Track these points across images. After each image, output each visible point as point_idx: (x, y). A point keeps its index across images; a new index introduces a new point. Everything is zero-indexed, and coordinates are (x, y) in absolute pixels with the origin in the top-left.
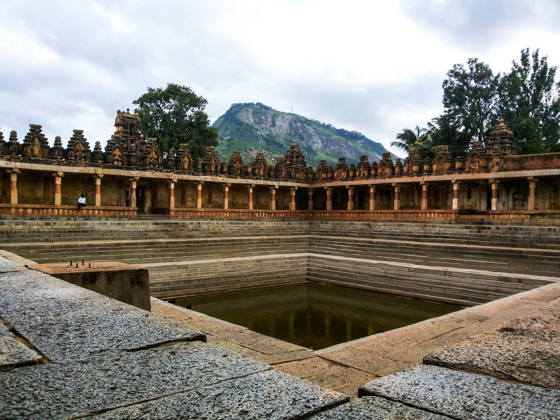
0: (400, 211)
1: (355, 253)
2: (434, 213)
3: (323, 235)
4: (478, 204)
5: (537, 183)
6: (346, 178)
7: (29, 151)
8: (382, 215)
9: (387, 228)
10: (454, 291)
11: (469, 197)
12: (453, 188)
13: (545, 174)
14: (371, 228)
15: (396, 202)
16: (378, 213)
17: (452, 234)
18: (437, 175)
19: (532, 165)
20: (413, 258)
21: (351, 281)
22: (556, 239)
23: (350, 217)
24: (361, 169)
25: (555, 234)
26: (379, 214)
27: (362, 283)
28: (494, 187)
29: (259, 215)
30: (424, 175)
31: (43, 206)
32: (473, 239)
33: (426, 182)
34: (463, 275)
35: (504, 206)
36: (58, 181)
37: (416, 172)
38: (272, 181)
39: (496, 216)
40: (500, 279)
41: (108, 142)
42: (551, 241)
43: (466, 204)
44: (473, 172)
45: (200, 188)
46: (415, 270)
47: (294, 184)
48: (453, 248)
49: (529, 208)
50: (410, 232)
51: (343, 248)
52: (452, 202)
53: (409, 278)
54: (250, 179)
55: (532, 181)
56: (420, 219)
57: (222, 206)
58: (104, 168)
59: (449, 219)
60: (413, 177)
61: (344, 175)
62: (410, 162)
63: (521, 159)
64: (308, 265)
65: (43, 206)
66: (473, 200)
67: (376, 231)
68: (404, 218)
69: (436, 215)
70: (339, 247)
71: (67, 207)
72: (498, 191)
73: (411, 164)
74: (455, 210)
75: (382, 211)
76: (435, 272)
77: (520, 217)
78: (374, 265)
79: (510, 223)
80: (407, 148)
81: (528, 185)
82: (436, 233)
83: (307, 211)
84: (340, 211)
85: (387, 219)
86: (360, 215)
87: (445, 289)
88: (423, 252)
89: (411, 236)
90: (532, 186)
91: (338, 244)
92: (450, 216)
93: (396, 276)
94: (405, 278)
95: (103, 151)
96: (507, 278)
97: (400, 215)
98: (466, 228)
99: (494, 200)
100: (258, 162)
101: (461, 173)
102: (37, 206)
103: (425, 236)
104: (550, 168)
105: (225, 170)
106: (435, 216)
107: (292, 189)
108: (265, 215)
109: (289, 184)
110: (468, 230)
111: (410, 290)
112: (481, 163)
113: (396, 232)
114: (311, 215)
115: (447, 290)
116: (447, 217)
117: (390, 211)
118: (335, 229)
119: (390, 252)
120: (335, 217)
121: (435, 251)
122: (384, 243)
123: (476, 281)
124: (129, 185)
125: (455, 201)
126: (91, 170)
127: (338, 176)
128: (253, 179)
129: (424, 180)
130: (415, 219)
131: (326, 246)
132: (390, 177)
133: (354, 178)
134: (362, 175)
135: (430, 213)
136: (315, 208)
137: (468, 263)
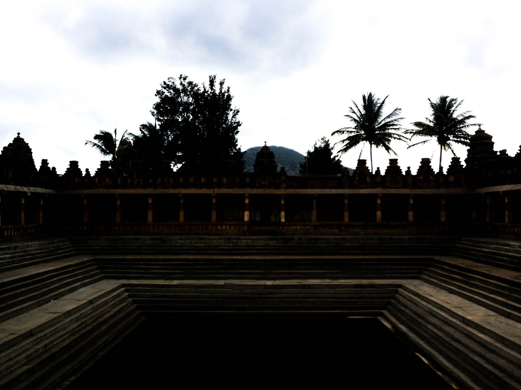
2: (226, 225)
8: (164, 228)
18: (228, 188)
26: (161, 227)
29: (7, 233)
30: (214, 188)
33: (217, 194)
39: (285, 228)
40: (355, 286)
46: (272, 287)
47: (44, 191)
50: (217, 246)
51: (153, 269)
52: (244, 214)
60: (201, 188)
64: (129, 296)
67: (175, 246)
69: (228, 227)
74: (247, 222)
80: (102, 150)
82: (245, 246)
90: (314, 202)
93: (257, 296)
98: (271, 239)
99: (283, 214)
108: (14, 233)
110: (275, 242)
113: (200, 246)
125: (247, 214)
133: (124, 186)
135: (222, 225)
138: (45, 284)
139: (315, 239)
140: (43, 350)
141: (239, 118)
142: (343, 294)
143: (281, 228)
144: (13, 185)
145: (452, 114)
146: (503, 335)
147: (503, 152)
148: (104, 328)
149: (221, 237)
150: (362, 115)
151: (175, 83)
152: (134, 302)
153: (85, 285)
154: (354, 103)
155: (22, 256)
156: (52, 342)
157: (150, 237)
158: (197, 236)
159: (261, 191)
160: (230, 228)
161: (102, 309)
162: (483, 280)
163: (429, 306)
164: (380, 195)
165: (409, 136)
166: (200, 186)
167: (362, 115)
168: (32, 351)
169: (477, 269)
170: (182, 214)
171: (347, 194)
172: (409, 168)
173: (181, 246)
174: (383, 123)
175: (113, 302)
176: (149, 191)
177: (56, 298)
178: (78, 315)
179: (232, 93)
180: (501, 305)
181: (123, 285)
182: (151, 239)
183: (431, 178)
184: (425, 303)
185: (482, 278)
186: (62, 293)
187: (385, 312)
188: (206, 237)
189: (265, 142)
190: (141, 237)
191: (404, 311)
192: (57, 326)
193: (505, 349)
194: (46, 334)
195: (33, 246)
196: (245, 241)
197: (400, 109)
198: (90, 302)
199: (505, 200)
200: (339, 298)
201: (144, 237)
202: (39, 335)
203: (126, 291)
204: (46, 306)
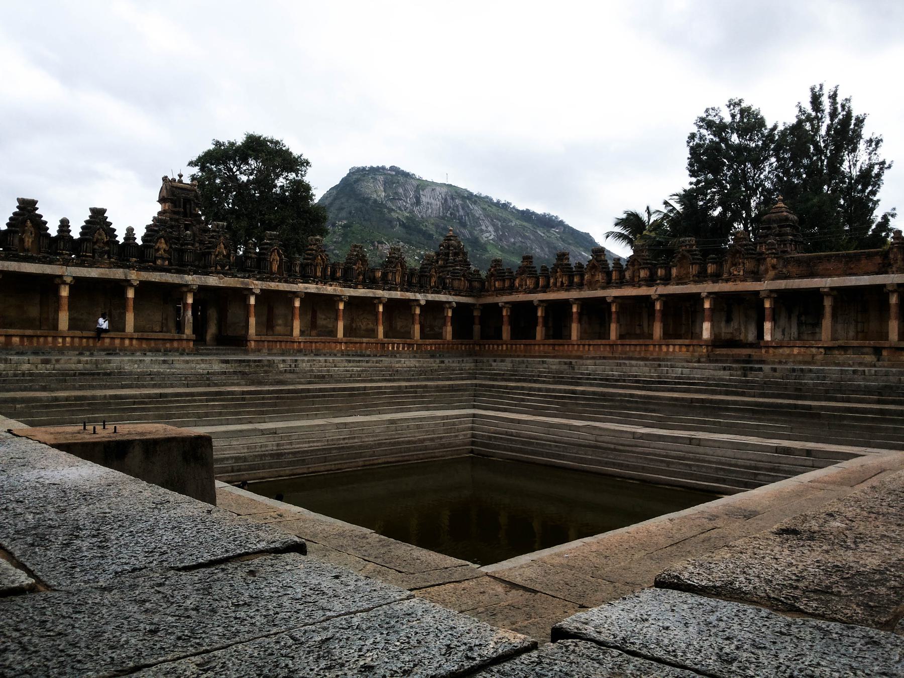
0: (619, 342)
1: (548, 409)
2: (674, 345)
3: (496, 380)
4: (743, 330)
5: (835, 299)
7: (16, 241)
8: (591, 348)
9: (599, 369)
10: (704, 470)
11: (729, 320)
12: (703, 305)
13: (849, 284)
14: (573, 368)
15: (613, 327)
16: (584, 345)
18: (677, 284)
19: (828, 270)
20: (641, 417)
22: (865, 386)
23: (540, 352)
25: (864, 379)
26: (587, 347)
27: (559, 457)
28: (767, 305)
29: (393, 348)
30: (658, 284)
31: (39, 332)
32: (736, 387)
33: (661, 296)
34: (717, 444)
35: (784, 334)
36: (65, 292)
37: (645, 280)
38: (415, 292)
39: (771, 350)
40: (777, 450)
41: (148, 227)
42: (857, 390)
43: (723, 330)
44: (735, 281)
45: (297, 304)
47: (450, 298)
50: (636, 376)
51: (528, 400)
53: (634, 449)
54: (379, 289)
55: (827, 294)
56: (652, 355)
57: (333, 332)
58: (140, 269)
59: (696, 354)
60: (639, 287)
61: (530, 283)
62: (636, 263)
63: (810, 259)
64: (472, 429)
65: (39, 332)
66: (734, 324)
67: (582, 374)
68: (625, 353)
69: (677, 348)
70: (523, 400)
71: (78, 333)
72: (774, 310)
73: (636, 267)
74: (706, 341)
75: (591, 343)
76: (675, 439)
77: (808, 351)
78: (577, 428)
79: (794, 362)
80: (630, 242)
81: (822, 301)
82: (676, 378)
83: (471, 341)
84: (524, 341)
85: (598, 354)
86: (557, 348)
87: (690, 466)
88: (656, 407)
89: (637, 381)
90: (828, 303)
91: (520, 394)
92: (699, 349)
93: (612, 446)
94: (627, 448)
95: (139, 242)
97: (620, 348)
98: (724, 369)
99: (768, 326)
101: (717, 282)
102: (29, 332)
103: (660, 383)
105: (339, 274)
106: (676, 350)
107: (447, 306)
108: (403, 348)
109: (442, 297)
110: (727, 372)
111: (635, 468)
113: (613, 375)
114: (477, 348)
115: (693, 468)
116: (694, 351)
117: (603, 342)
118: (516, 371)
119: (603, 407)
120: (516, 351)
121: (675, 405)
122: (594, 393)
123: (739, 454)
124: (182, 299)
125: (706, 326)
126: (118, 274)
127: (521, 285)
128: (384, 290)
129: (658, 292)
130: (643, 355)
131: (501, 398)
132: (604, 288)
133: (546, 289)
134: (559, 284)
135: (668, 345)
136: (484, 336)
137: (727, 425)
141: (883, 154)
151: (722, 114)
157: (557, 360)
171: (892, 285)
176: (573, 294)
182: (560, 363)
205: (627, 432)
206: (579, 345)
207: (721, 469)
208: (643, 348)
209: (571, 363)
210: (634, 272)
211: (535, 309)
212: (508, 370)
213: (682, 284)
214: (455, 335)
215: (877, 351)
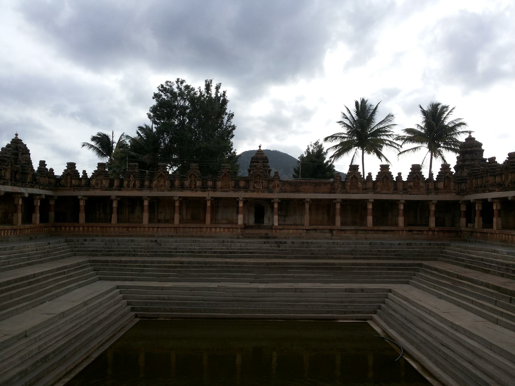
0: (182, 225)
1: (168, 276)
3: (96, 255)
6: (109, 187)
8: (159, 230)
17: (256, 249)
18: (222, 191)
21: (200, 311)
24: (132, 179)
26: (156, 229)
29: (4, 234)
35: (269, 221)
38: (19, 186)
39: (278, 231)
40: (346, 290)
46: (264, 290)
48: (274, 264)
49: (305, 224)
50: (211, 249)
51: (147, 271)
55: (307, 202)
60: (196, 191)
61: (106, 183)
64: (124, 298)
67: (169, 248)
69: (222, 229)
70: (143, 271)
73: (193, 179)
78: (215, 289)
81: (304, 204)
82: (239, 249)
84: (101, 224)
86: (130, 229)
87: (306, 305)
90: (307, 206)
91: (140, 266)
93: (249, 299)
96: (352, 289)
98: (265, 243)
100: (5, 161)
101: (247, 192)
103: (230, 253)
104: (319, 193)
107: (38, 197)
108: (11, 233)
110: (269, 245)
112: (264, 184)
113: (194, 249)
118: (111, 248)
119: (211, 271)
122: (198, 263)
125: (240, 217)
127: (97, 184)
130: (199, 234)
132: (169, 191)
133: (121, 187)
134: (131, 185)
135: (216, 228)
138: (41, 285)
139: (308, 243)
140: (37, 352)
141: (233, 122)
142: (335, 298)
143: (274, 231)
144: (11, 185)
145: (443, 121)
146: (491, 341)
147: (492, 160)
148: (98, 329)
149: (215, 240)
150: (355, 121)
151: (173, 87)
152: (128, 304)
153: (80, 286)
154: (347, 109)
155: (19, 256)
156: (46, 343)
158: (192, 239)
159: (255, 195)
160: (224, 231)
161: (96, 311)
162: (471, 285)
163: (418, 311)
164: (372, 201)
165: (400, 142)
166: (195, 189)
167: (355, 121)
168: (26, 352)
169: (466, 275)
170: (177, 217)
172: (400, 174)
173: (176, 249)
174: (376, 128)
175: (108, 304)
177: (51, 298)
178: (72, 316)
179: (228, 96)
180: (489, 311)
181: (118, 287)
182: (147, 241)
183: (421, 184)
184: (414, 308)
185: (470, 284)
186: (57, 294)
187: (374, 316)
188: (201, 239)
189: (260, 147)
190: (136, 239)
191: (394, 316)
192: (52, 327)
193: (493, 355)
194: (40, 335)
195: (30, 247)
196: (239, 244)
197: (392, 116)
198: (85, 304)
199: (493, 207)
200: (331, 302)
201: (139, 239)
202: (33, 336)
203: (121, 292)
204: (41, 306)
205: (253, 288)
206: (149, 227)
207: (326, 305)
208: (199, 229)
209: (156, 241)
210: (191, 181)
211: (111, 202)
212: (103, 247)
213: (225, 191)
214: (41, 221)
215: (331, 231)
